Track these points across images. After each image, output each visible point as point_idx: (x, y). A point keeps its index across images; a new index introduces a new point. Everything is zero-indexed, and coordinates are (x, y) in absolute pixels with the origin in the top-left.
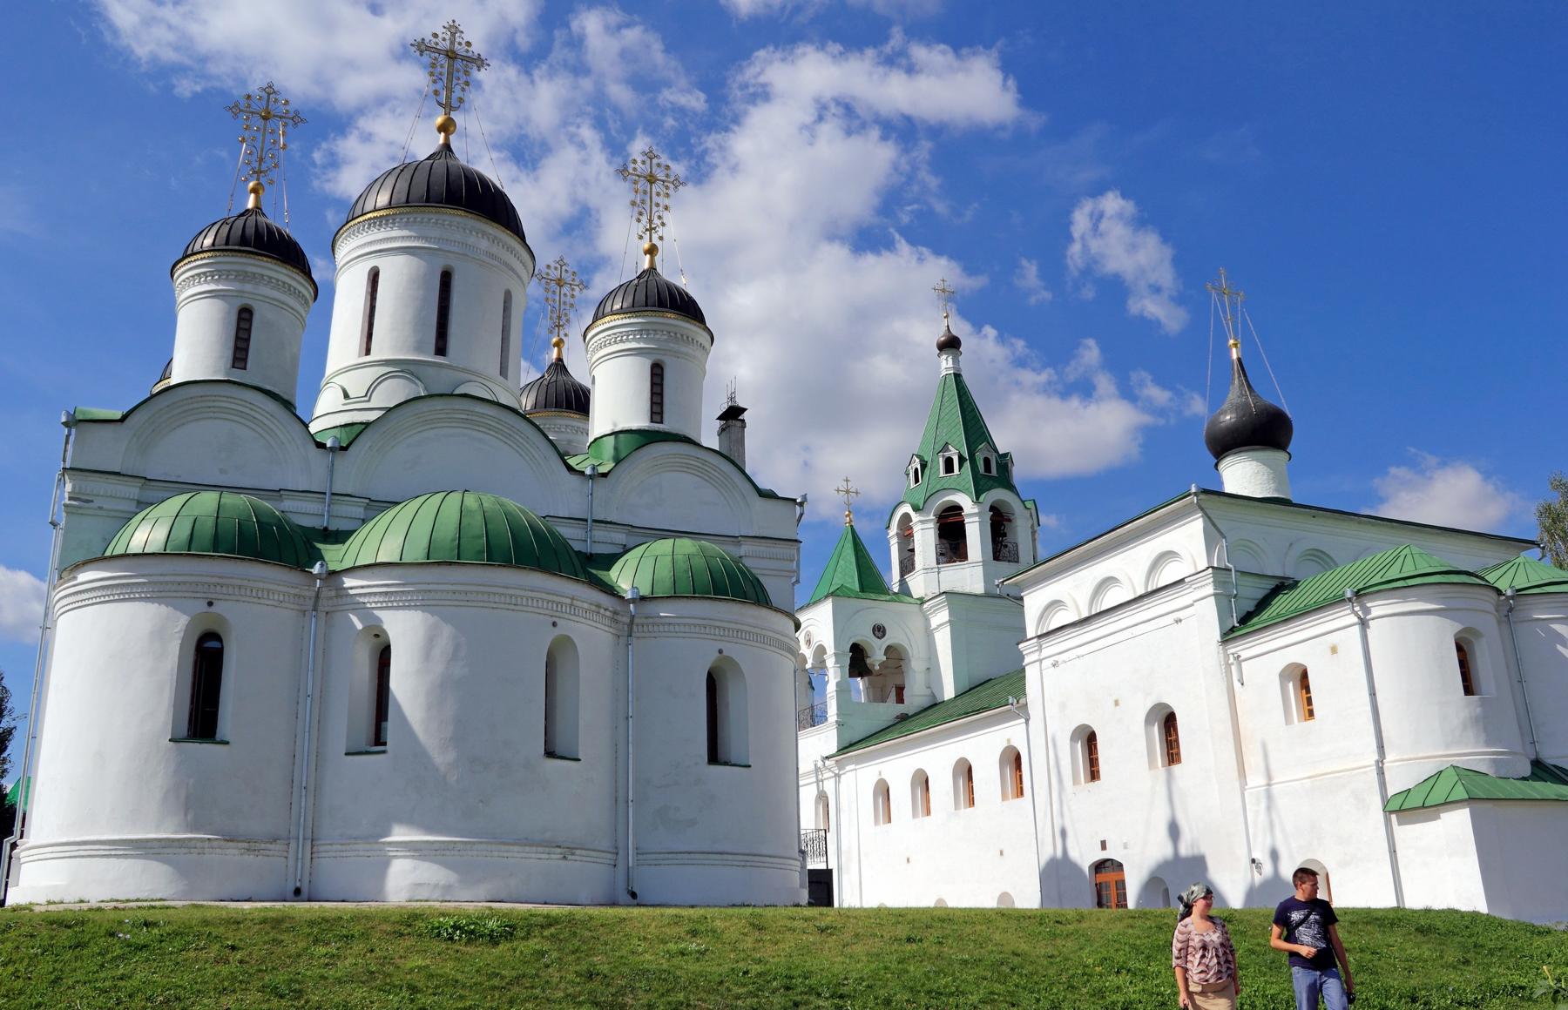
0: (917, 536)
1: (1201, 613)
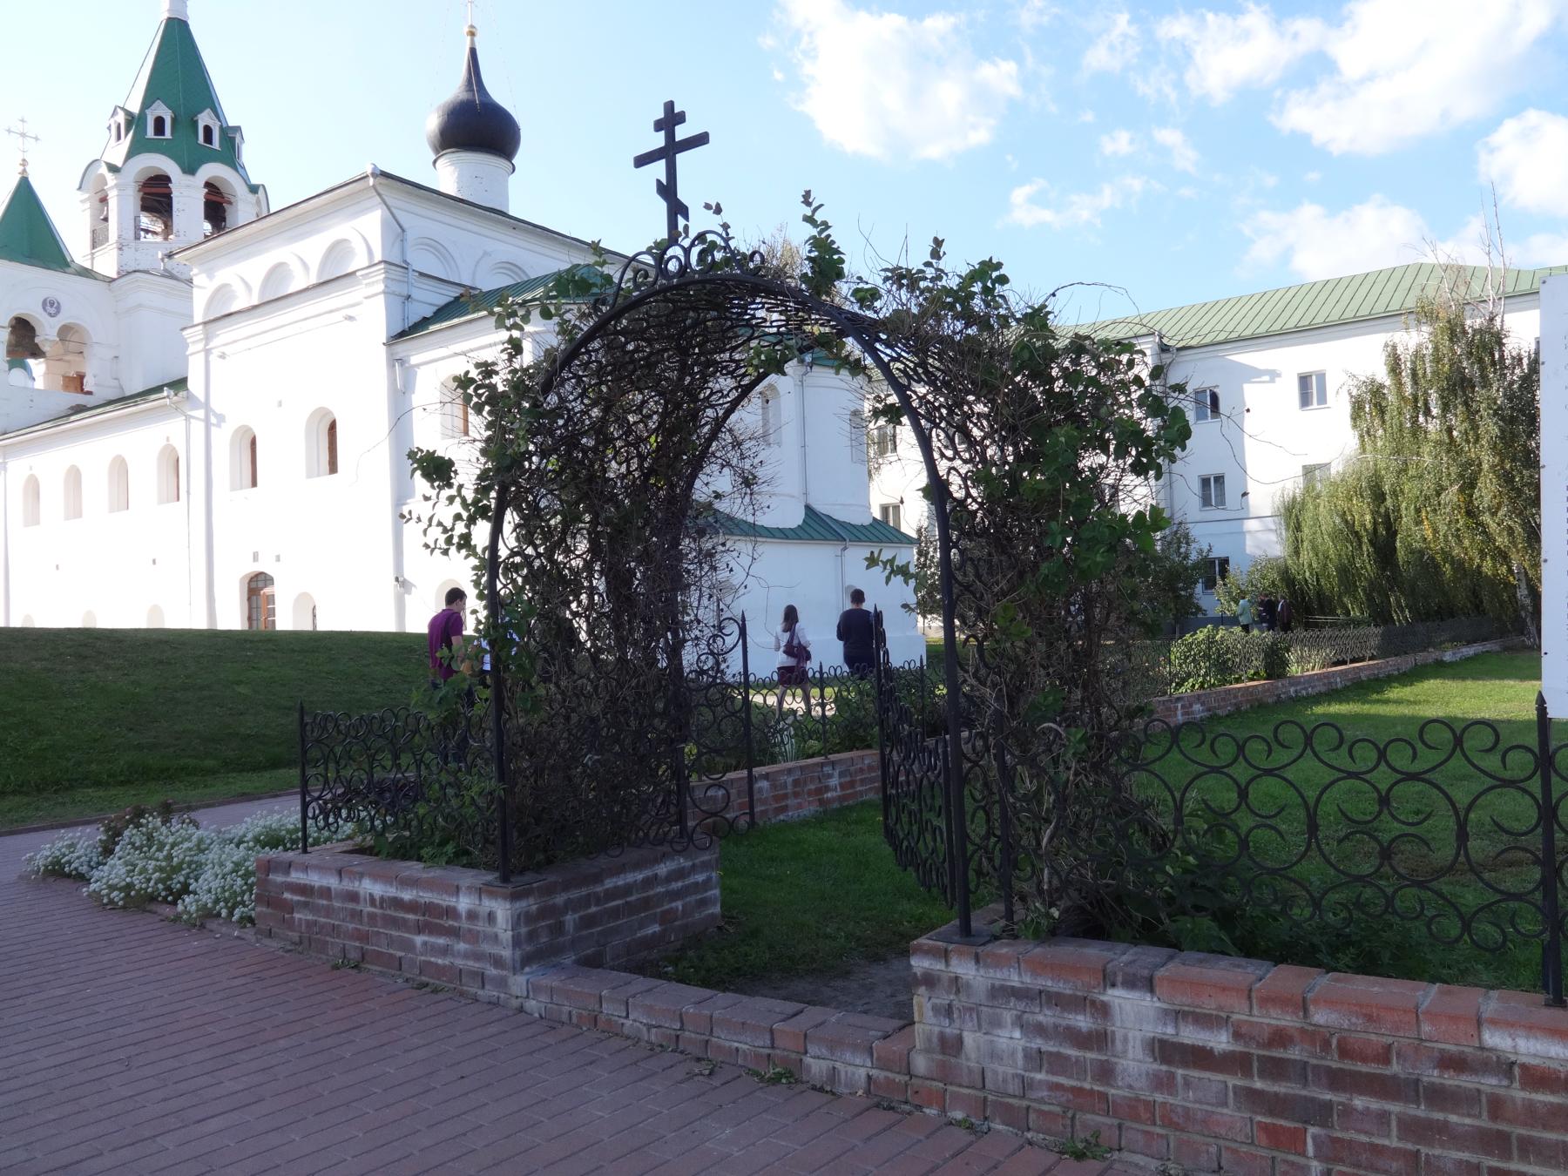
0: (113, 203)
1: (369, 311)
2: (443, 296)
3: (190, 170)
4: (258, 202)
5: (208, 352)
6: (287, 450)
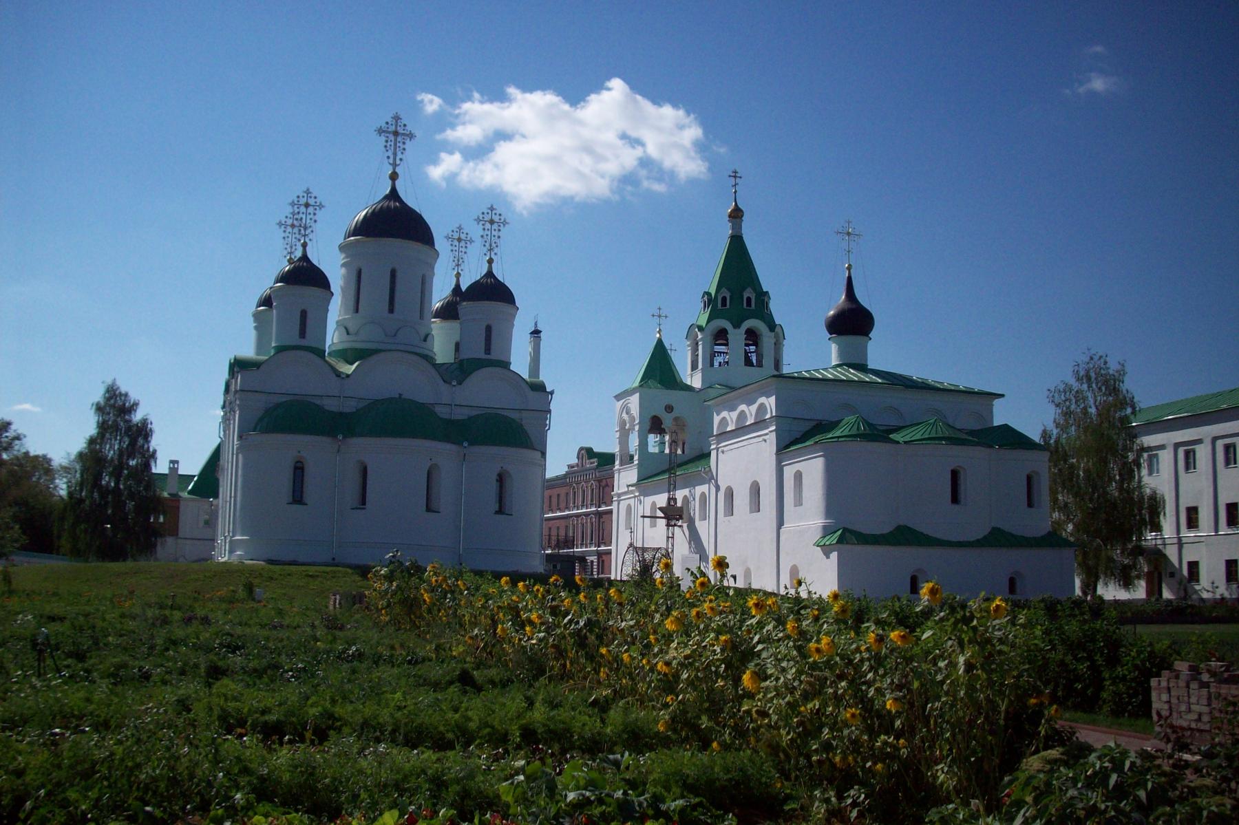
0: (700, 347)
2: (806, 427)
3: (737, 325)
4: (777, 337)
5: (717, 449)
6: (742, 500)
